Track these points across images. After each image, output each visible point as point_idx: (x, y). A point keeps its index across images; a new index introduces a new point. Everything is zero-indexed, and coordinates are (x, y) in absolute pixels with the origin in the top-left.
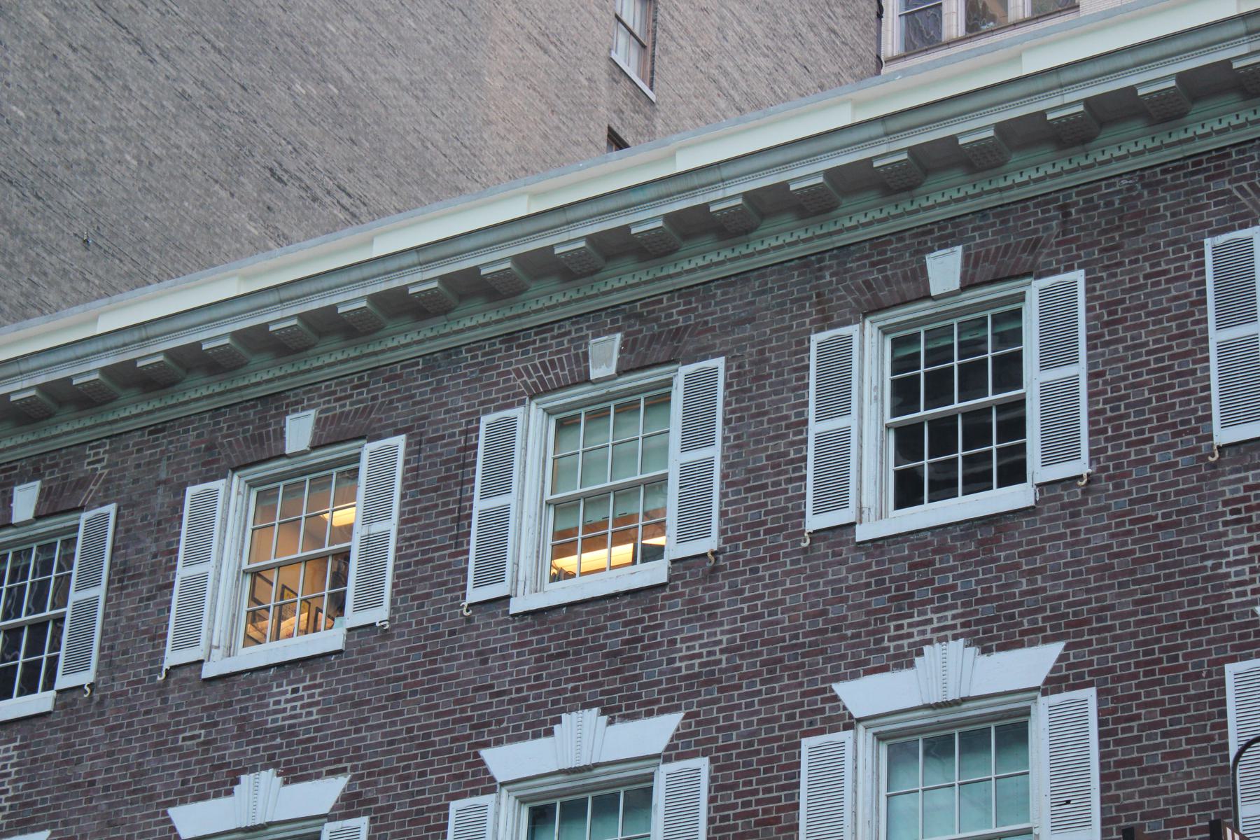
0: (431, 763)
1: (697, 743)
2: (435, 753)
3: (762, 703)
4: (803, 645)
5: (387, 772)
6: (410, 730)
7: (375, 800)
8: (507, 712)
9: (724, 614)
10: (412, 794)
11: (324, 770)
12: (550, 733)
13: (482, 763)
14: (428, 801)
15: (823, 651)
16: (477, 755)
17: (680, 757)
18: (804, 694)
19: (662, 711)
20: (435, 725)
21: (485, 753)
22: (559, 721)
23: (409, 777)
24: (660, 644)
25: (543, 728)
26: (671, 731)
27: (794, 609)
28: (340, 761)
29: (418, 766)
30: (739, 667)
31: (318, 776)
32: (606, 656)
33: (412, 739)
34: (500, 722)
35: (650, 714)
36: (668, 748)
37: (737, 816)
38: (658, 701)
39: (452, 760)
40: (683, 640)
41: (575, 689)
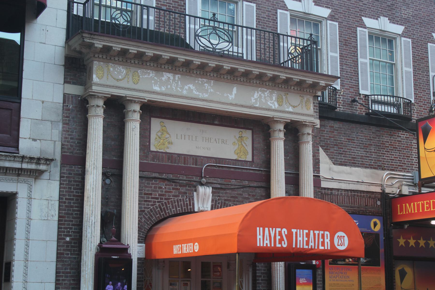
0: (351, 15)
1: (408, 35)
2: (351, 13)
3: (420, 31)
4: (426, 21)
5: (340, 13)
6: (345, 4)
7: (338, 19)
8: (367, 10)
9: (411, 7)
10: (347, 21)
11: (325, 5)
12: (377, 19)
13: (362, 20)
14: (351, 25)
15: (430, 25)
16: (361, 18)
17: (404, 37)
18: (427, 33)
19: (400, 24)
20: (351, 6)
21: (363, 18)
22: (380, 18)
23: (346, 16)
24: (398, 8)
25: (376, 17)
26: (402, 30)
27: (424, 12)
28: (328, 5)
29: (348, 14)
30: (414, 21)
31: (323, 7)
32: (388, 6)
33: (346, 7)
34: (365, 12)
35: (397, 24)
36: (402, 34)
37: (417, 55)
38: (399, 22)
39: (355, 16)
40: (403, 9)
41: (381, 11)
